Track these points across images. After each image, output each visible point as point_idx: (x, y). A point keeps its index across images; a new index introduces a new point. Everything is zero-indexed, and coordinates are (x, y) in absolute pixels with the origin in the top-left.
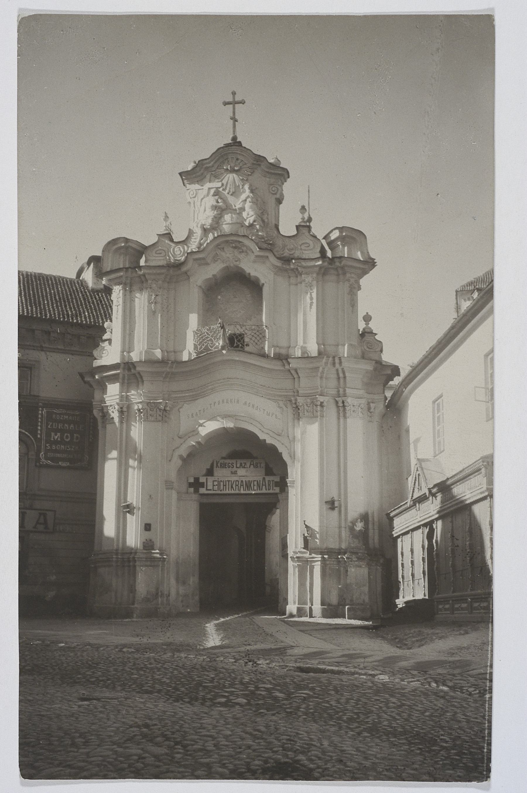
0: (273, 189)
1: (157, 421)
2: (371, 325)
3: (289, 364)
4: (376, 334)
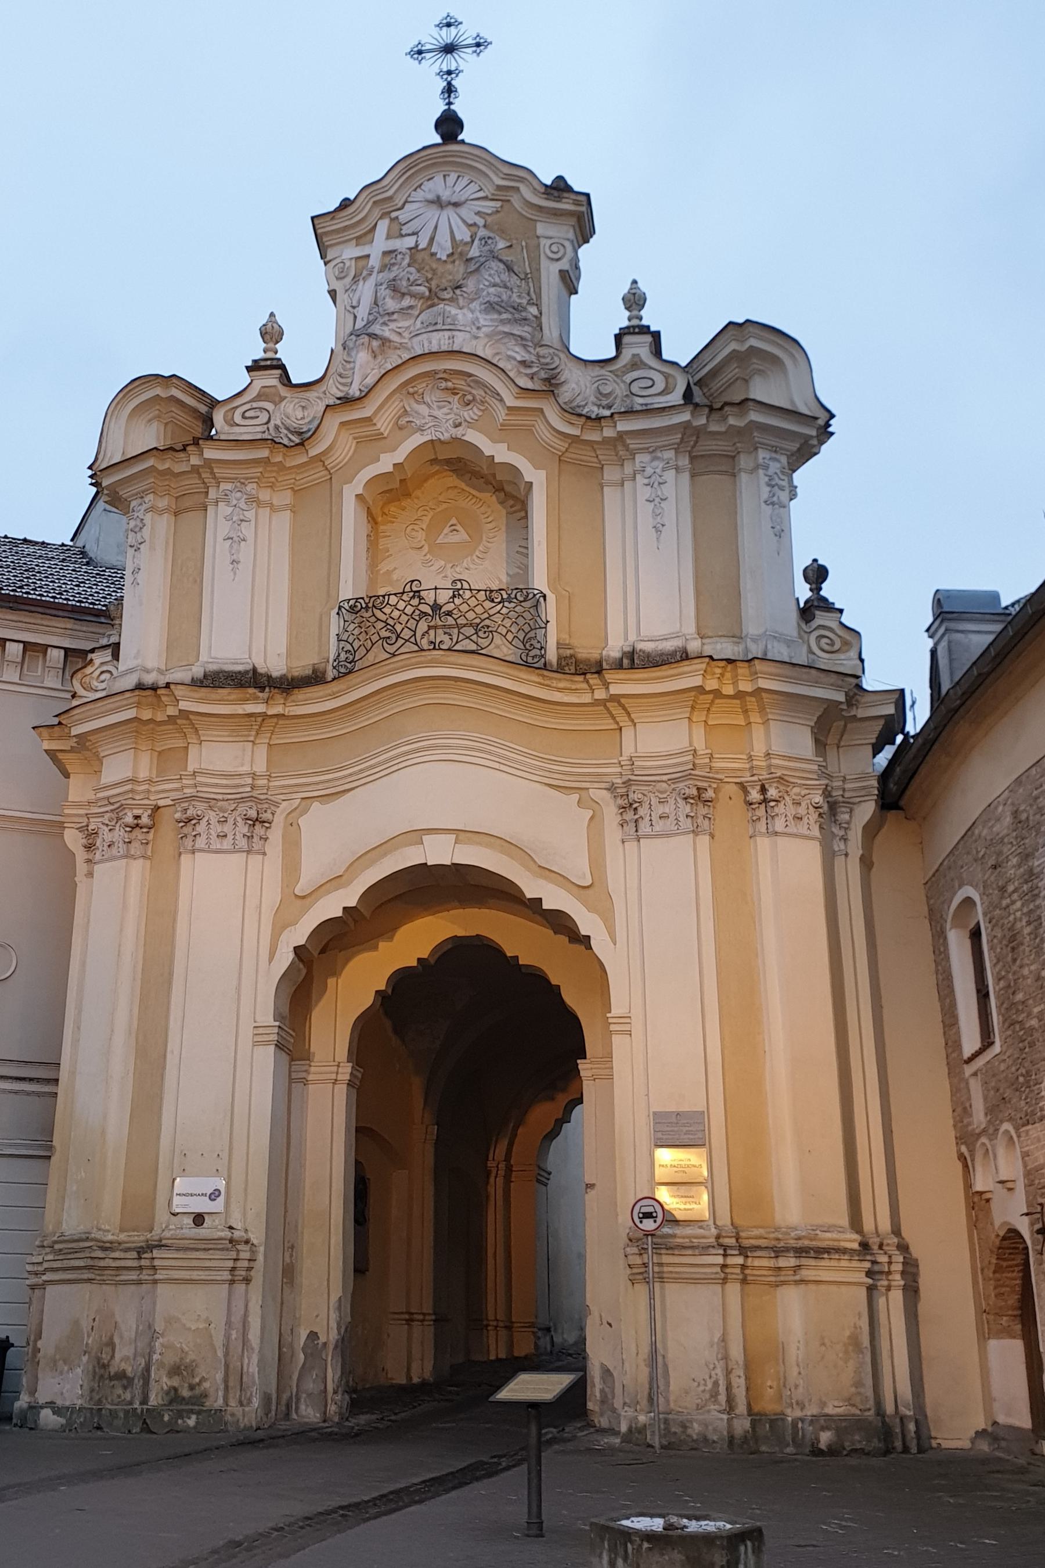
0: (554, 248)
1: (235, 851)
2: (827, 590)
3: (606, 685)
4: (841, 611)
